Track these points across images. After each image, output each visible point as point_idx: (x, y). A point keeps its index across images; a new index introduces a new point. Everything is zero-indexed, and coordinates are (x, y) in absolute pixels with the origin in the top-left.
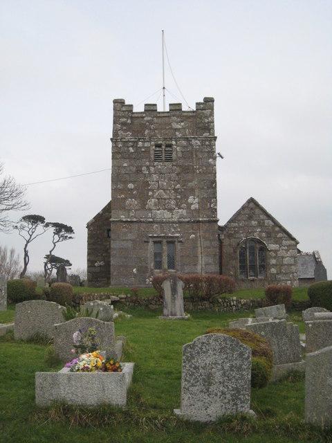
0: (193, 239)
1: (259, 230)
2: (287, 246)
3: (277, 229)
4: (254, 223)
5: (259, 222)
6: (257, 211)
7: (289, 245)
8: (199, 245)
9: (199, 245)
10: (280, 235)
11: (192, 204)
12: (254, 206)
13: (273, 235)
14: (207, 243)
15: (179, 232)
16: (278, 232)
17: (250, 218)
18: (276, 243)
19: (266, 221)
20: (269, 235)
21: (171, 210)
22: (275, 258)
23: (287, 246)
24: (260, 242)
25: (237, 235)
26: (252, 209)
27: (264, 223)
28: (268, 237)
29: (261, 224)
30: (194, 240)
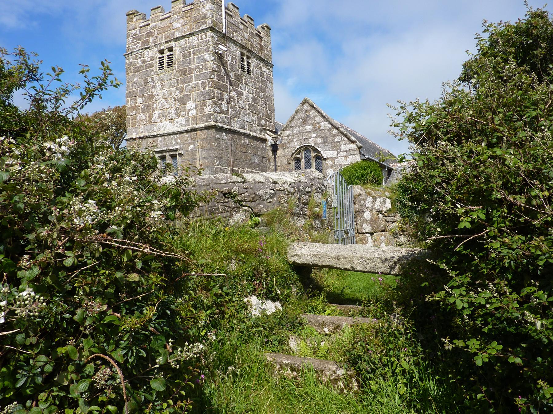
0: (192, 151)
1: (314, 135)
2: (346, 151)
3: (335, 131)
4: (309, 128)
5: (314, 127)
6: (313, 113)
7: (349, 150)
8: (198, 156)
9: (198, 155)
10: (338, 139)
11: (189, 110)
12: (309, 107)
13: (330, 139)
14: (205, 153)
15: (180, 144)
16: (335, 136)
17: (305, 122)
18: (333, 148)
19: (322, 124)
20: (325, 141)
21: (171, 120)
22: (332, 167)
23: (346, 151)
24: (316, 150)
25: (292, 145)
26: (306, 111)
27: (320, 126)
28: (324, 143)
29: (317, 128)
30: (193, 151)
